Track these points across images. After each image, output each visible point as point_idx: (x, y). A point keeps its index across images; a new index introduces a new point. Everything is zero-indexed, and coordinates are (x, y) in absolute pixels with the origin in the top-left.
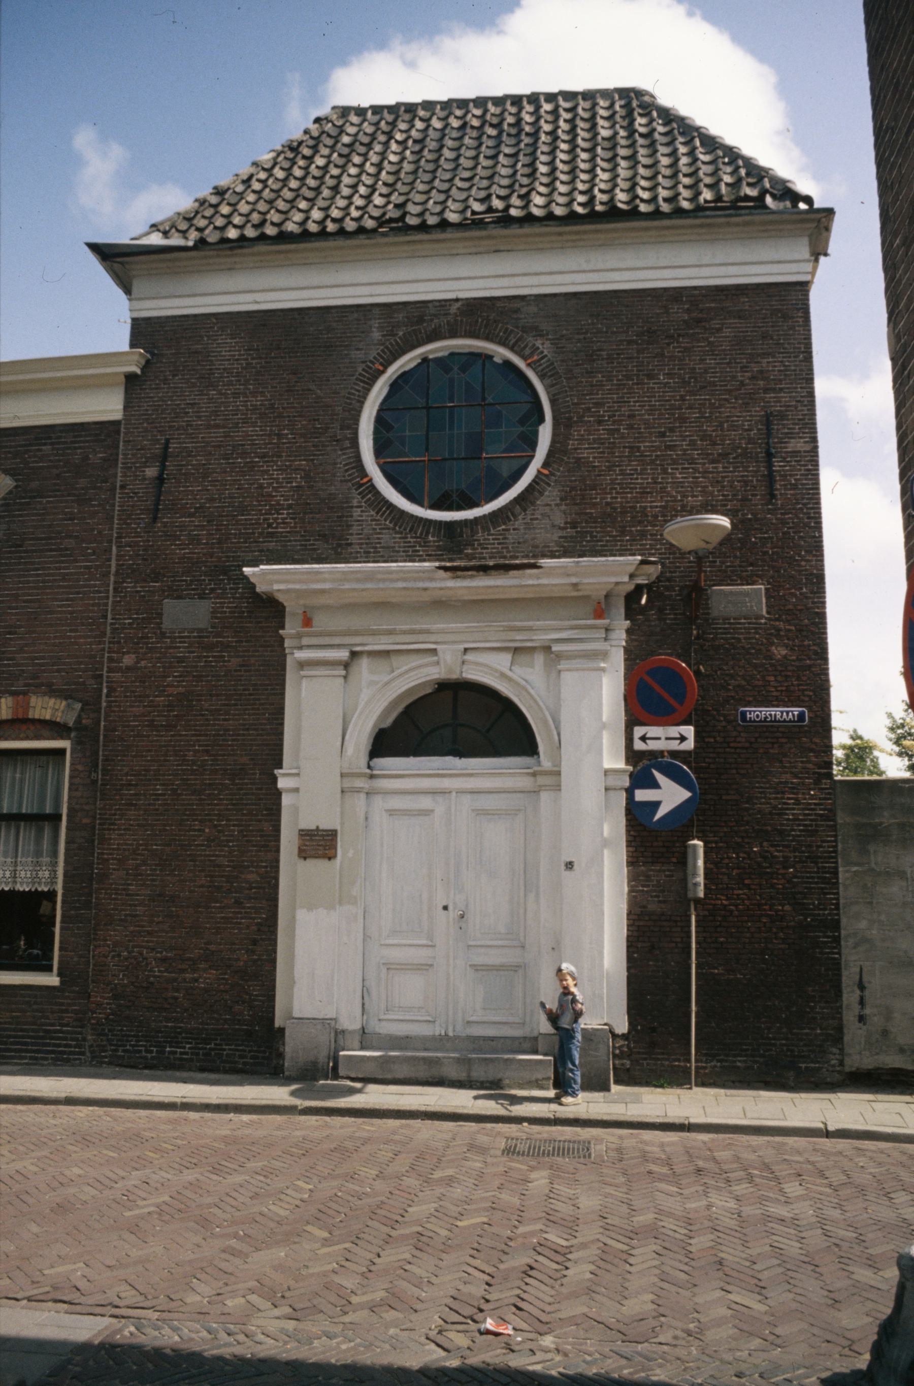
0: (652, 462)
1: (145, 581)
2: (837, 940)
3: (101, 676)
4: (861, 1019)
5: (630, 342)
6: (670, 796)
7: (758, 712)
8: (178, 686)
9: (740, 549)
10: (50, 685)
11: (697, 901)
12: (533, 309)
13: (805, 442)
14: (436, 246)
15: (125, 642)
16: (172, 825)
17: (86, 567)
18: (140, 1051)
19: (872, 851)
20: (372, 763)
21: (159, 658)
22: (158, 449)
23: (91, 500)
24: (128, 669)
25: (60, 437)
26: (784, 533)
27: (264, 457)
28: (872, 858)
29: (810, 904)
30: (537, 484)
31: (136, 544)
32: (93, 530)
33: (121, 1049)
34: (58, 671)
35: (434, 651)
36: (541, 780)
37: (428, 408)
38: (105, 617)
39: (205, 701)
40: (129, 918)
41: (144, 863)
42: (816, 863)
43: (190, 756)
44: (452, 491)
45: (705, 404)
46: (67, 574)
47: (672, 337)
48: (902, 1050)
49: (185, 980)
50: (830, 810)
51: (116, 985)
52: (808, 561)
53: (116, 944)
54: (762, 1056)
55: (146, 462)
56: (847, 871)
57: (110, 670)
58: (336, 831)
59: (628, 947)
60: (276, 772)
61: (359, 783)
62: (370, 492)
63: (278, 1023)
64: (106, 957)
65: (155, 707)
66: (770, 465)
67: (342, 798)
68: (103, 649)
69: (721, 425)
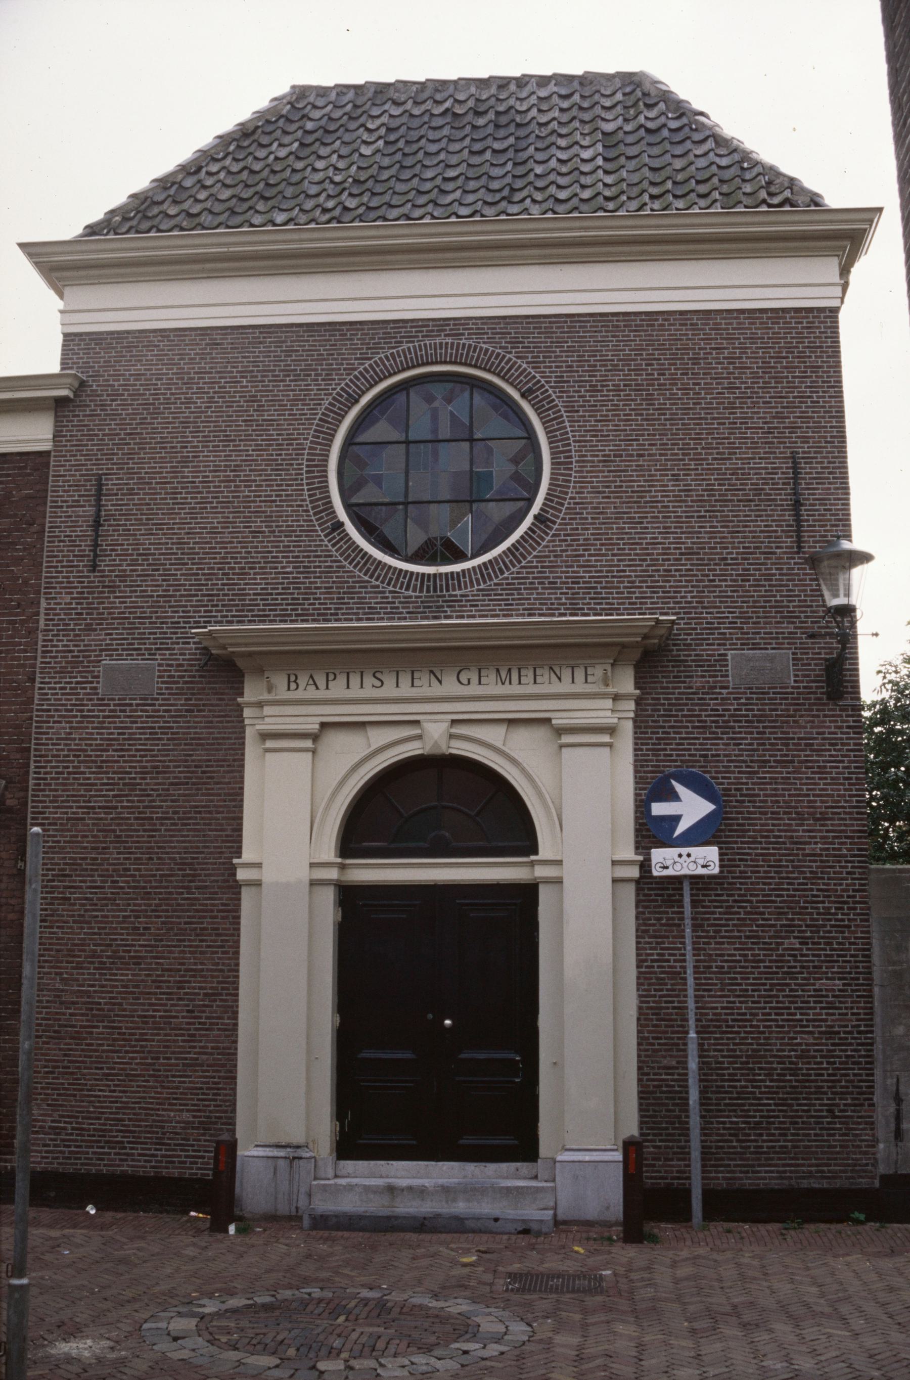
3: (28, 750)
17: (9, 622)
35: (417, 722)
44: (436, 538)
67: (310, 892)
68: (31, 718)
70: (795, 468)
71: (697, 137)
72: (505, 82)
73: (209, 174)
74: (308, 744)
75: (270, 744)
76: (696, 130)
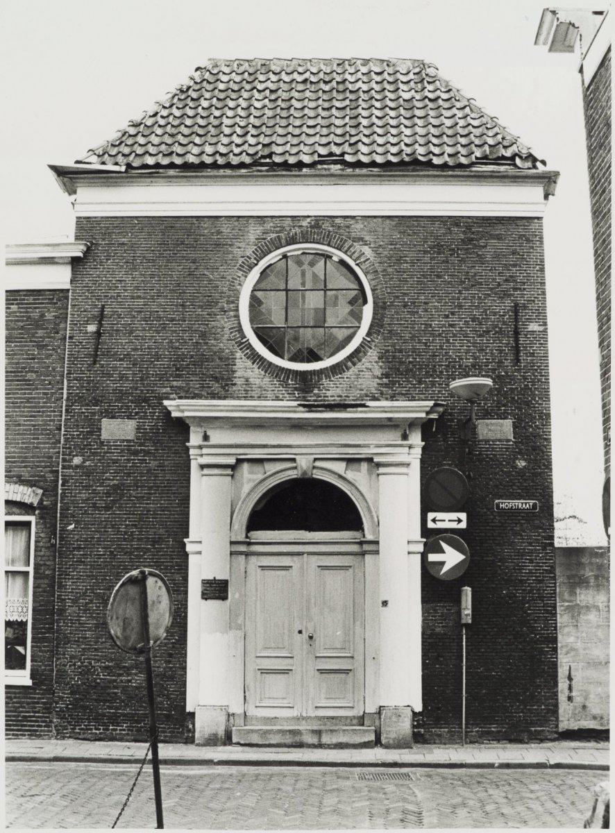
0: (440, 335)
1: (88, 405)
2: (555, 650)
3: (57, 471)
4: (570, 699)
5: (425, 252)
6: (451, 558)
7: (506, 504)
8: (113, 480)
9: (497, 395)
10: (19, 477)
11: (466, 625)
12: (359, 226)
13: (540, 325)
14: (295, 179)
15: (74, 448)
16: (110, 576)
17: (44, 394)
18: (91, 729)
19: (578, 593)
20: (249, 535)
21: (99, 460)
22: (96, 312)
23: (47, 345)
24: (77, 467)
25: (24, 300)
26: (525, 385)
27: (173, 321)
28: (578, 598)
29: (538, 627)
30: (363, 347)
31: (81, 379)
32: (49, 367)
33: (77, 728)
34: (25, 467)
35: (294, 460)
36: (366, 547)
37: (287, 290)
38: (60, 429)
39: (134, 490)
40: (81, 640)
41: (91, 602)
42: (543, 601)
43: (123, 529)
45: (474, 297)
46: (31, 398)
47: (453, 250)
48: (595, 718)
49: (122, 681)
50: (552, 567)
51: (73, 685)
52: (539, 404)
53: (72, 657)
54: (507, 724)
55: (88, 321)
56: (562, 606)
57: (64, 467)
58: (227, 581)
59: (423, 656)
60: (185, 540)
61: (243, 548)
62: (248, 349)
63: (189, 709)
64: (65, 666)
65: (97, 494)
66: (517, 340)
68: (59, 453)
69: (485, 311)
70: (516, 312)
71: (458, 105)
72: (341, 62)
73: (162, 117)
74: (229, 472)
75: (206, 471)
76: (459, 100)
